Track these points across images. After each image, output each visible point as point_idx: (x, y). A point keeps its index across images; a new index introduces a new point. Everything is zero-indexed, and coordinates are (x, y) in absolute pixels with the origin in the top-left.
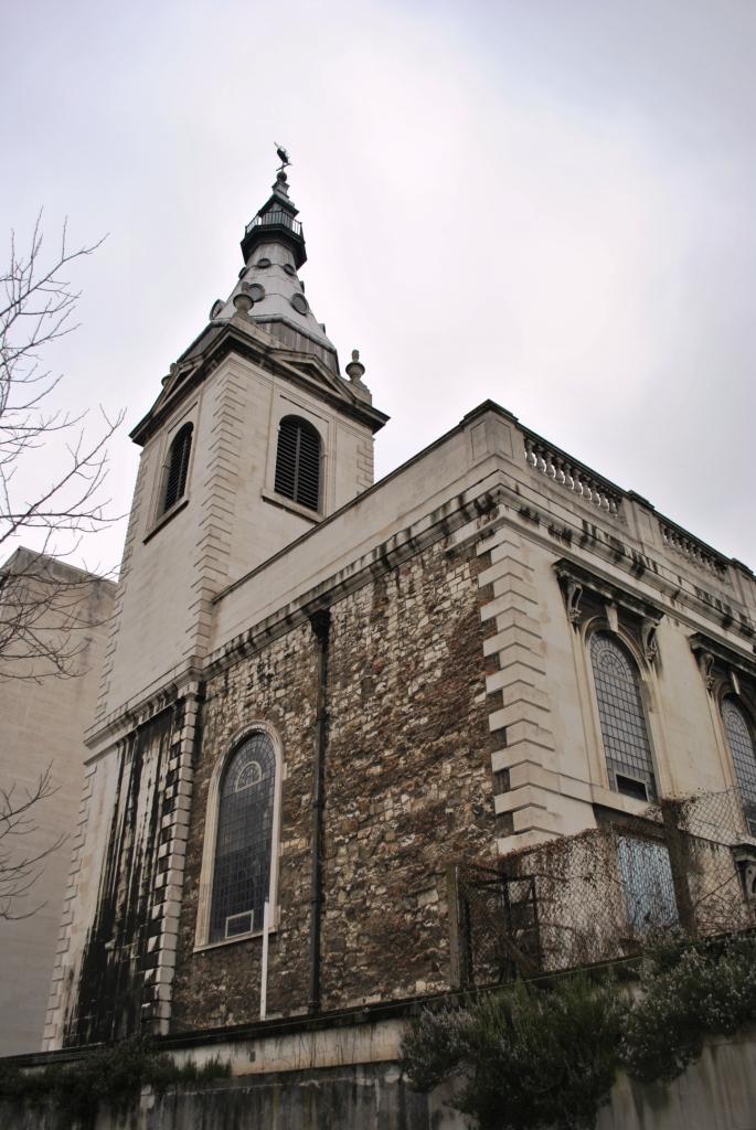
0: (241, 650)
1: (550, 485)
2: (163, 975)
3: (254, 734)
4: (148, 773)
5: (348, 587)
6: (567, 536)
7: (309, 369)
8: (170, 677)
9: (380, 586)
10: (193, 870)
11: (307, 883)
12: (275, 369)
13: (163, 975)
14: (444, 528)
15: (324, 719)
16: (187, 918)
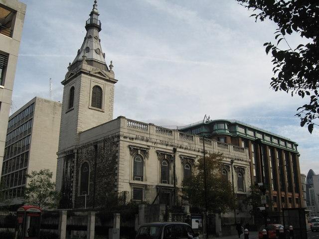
0: (84, 147)
1: (132, 129)
2: (73, 199)
3: (86, 162)
5: (100, 142)
6: (133, 139)
7: (99, 73)
8: (72, 148)
9: (104, 142)
10: (77, 183)
11: (93, 189)
12: (91, 75)
13: (73, 199)
14: (113, 138)
15: (96, 164)
16: (76, 191)
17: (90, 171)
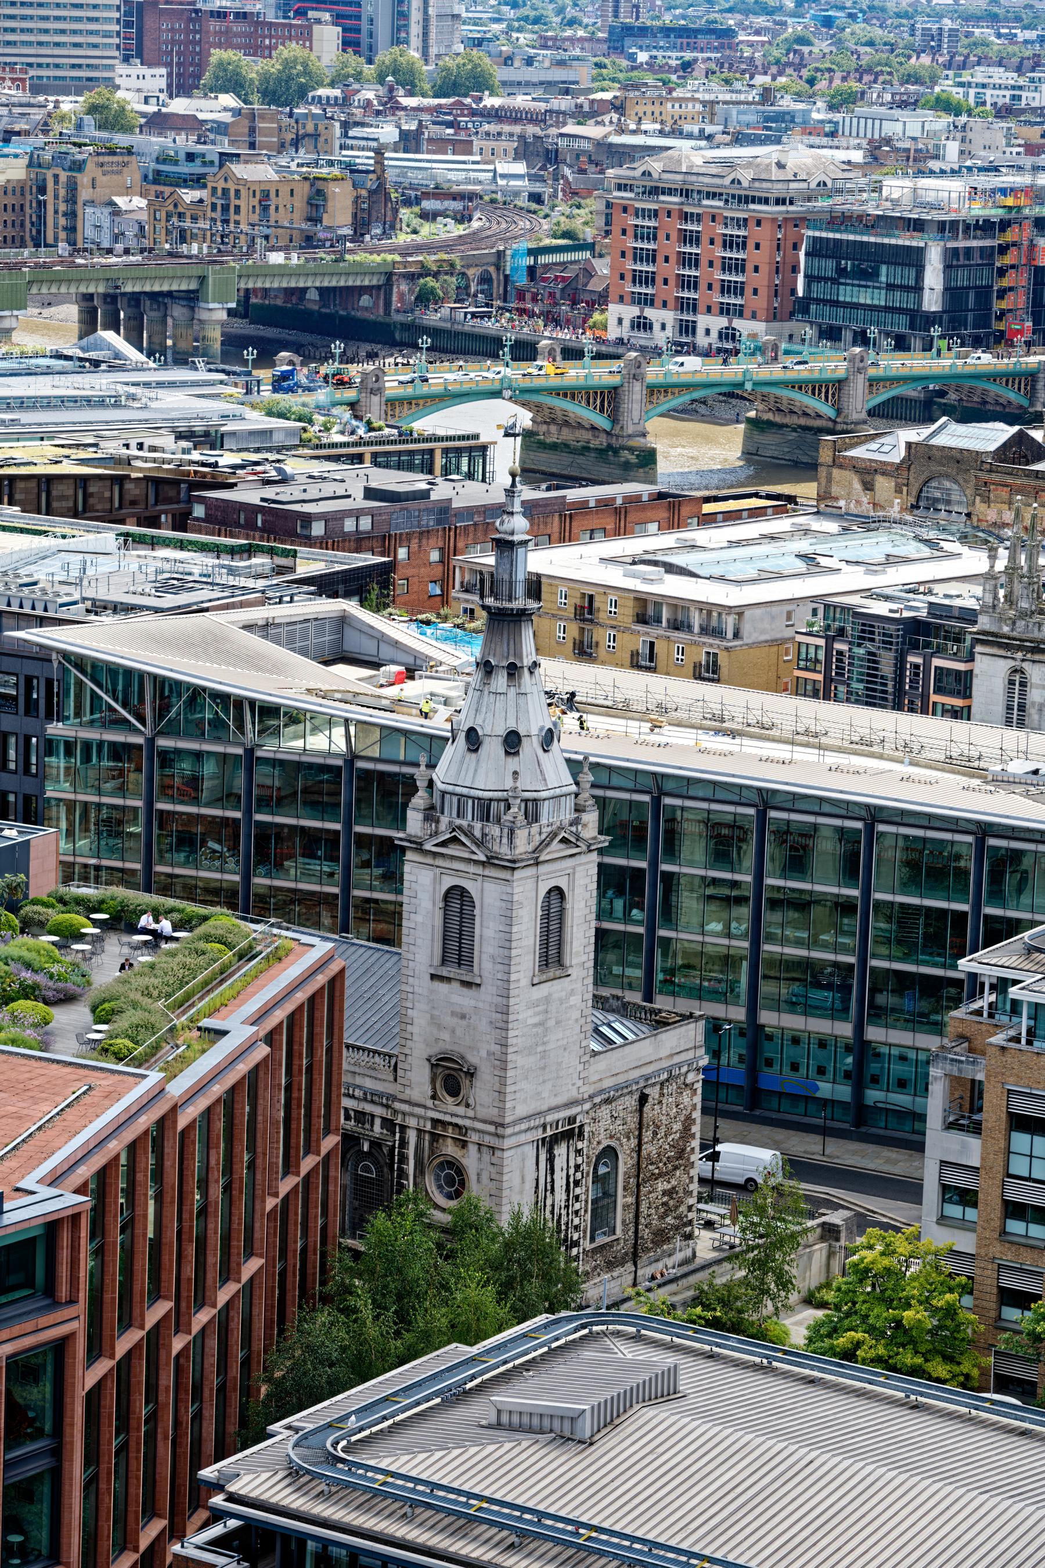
4: (560, 1162)
9: (661, 1089)
15: (640, 1145)
17: (622, 1169)
